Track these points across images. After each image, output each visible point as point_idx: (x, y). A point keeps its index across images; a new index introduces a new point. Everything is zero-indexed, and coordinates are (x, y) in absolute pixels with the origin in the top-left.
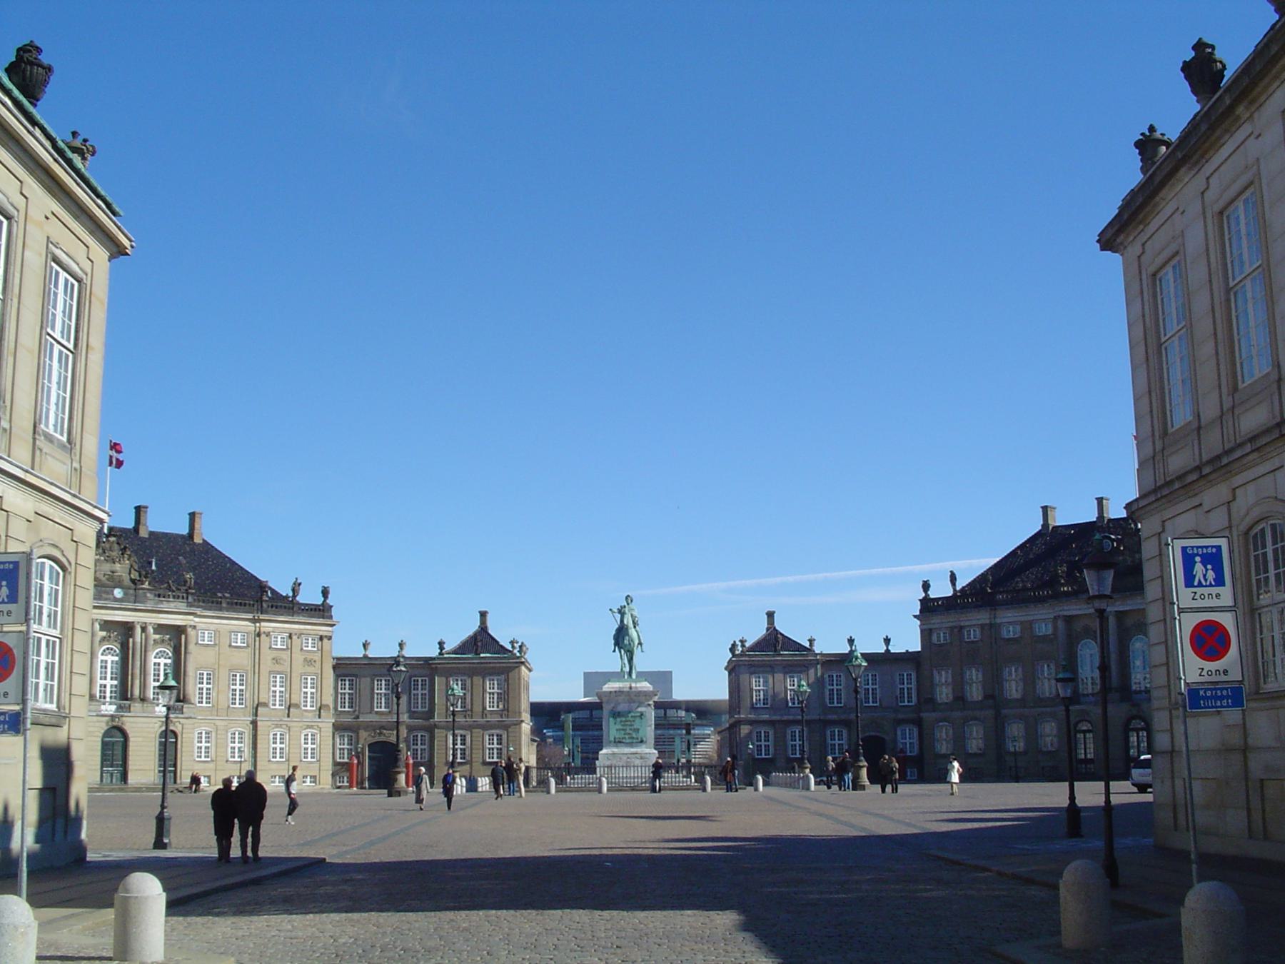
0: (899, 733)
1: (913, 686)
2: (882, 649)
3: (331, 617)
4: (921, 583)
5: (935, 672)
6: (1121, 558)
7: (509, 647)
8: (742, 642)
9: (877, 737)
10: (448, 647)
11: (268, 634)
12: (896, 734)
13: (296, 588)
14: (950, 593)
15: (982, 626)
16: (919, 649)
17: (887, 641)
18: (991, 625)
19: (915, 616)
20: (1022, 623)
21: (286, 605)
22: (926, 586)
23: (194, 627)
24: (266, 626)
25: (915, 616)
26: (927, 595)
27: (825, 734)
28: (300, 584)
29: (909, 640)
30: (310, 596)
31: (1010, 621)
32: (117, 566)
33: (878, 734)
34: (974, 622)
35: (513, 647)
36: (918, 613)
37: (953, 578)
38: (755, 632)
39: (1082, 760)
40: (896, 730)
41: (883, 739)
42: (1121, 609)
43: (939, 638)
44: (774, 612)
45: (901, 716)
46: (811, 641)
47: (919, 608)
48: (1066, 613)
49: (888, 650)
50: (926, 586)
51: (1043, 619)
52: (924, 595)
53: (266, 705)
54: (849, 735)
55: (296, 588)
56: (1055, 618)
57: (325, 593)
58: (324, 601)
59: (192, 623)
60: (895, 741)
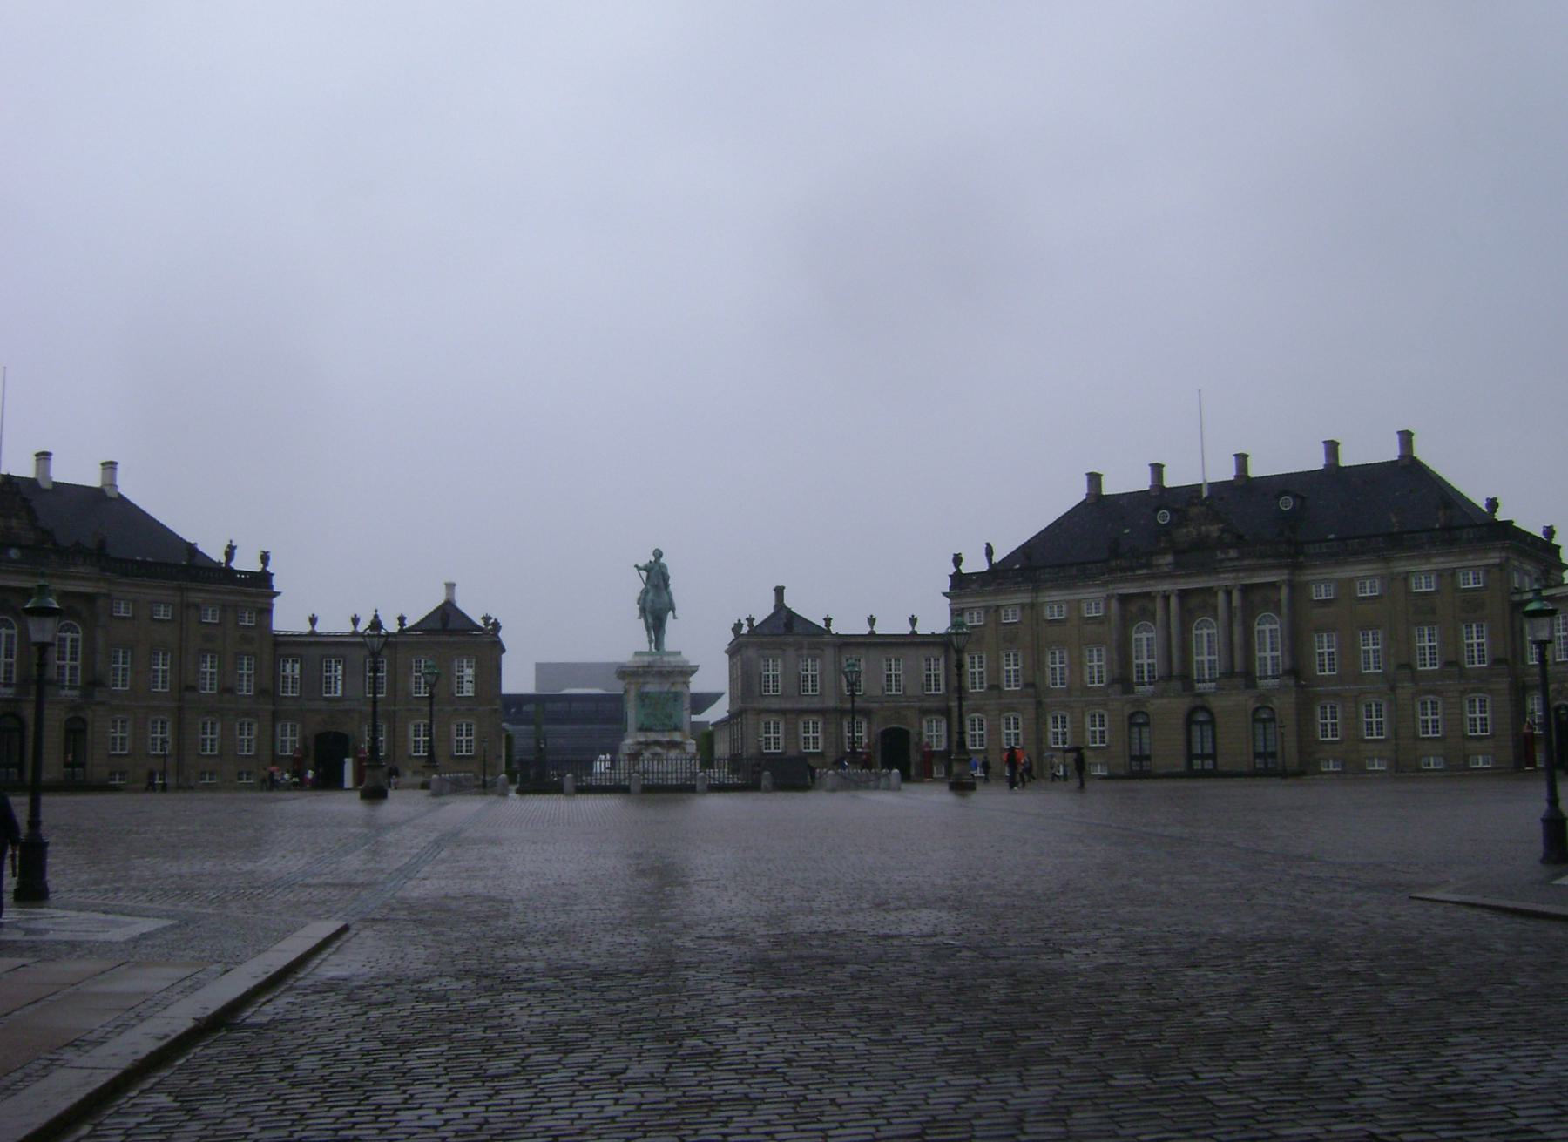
0: (925, 724)
3: (272, 587)
4: (952, 557)
6: (1185, 530)
7: (481, 623)
8: (750, 620)
10: (409, 623)
11: (197, 607)
12: (921, 728)
13: (230, 552)
14: (983, 566)
15: (1023, 606)
18: (1033, 606)
19: (944, 594)
20: (1068, 602)
21: (222, 574)
22: (957, 560)
23: (107, 596)
24: (195, 597)
25: (944, 594)
26: (959, 571)
27: (842, 724)
28: (235, 548)
29: (936, 620)
30: (246, 562)
31: (1055, 603)
32: (14, 523)
33: (902, 726)
34: (1015, 601)
35: (486, 624)
36: (948, 590)
37: (989, 551)
38: (763, 610)
40: (921, 723)
42: (1184, 587)
43: (974, 620)
44: (784, 588)
45: (926, 704)
46: (828, 621)
48: (1120, 592)
49: (914, 633)
50: (957, 560)
51: (1092, 600)
52: (954, 570)
53: (193, 688)
54: (869, 728)
55: (230, 552)
56: (1109, 597)
57: (265, 558)
58: (264, 569)
59: (104, 591)
60: (920, 734)
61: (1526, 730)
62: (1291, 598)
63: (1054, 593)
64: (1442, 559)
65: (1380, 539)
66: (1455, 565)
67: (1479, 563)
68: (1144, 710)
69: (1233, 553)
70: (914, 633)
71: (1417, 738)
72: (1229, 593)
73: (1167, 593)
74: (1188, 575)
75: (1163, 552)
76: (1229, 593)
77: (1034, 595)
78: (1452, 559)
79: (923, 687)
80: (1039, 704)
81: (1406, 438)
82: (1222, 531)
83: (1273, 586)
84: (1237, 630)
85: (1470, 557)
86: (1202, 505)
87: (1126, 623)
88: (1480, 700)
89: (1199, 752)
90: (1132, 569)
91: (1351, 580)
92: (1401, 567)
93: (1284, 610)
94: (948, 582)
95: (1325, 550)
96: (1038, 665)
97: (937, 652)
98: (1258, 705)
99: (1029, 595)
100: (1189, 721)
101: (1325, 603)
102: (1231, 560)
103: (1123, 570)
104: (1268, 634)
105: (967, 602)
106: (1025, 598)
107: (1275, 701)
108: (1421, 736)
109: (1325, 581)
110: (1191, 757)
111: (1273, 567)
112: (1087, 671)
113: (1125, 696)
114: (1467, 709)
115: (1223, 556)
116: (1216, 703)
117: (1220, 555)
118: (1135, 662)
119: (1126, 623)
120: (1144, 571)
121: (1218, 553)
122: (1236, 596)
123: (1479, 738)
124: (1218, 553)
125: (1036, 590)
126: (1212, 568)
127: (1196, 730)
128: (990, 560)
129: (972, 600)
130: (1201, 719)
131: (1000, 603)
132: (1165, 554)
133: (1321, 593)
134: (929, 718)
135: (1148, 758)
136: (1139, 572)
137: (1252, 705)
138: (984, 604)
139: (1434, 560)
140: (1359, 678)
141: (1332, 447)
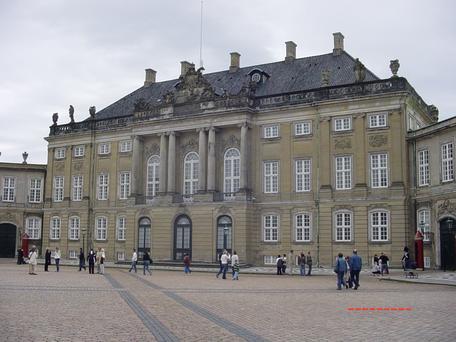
1: (41, 189)
2: (21, 161)
5: (55, 180)
6: (184, 92)
9: (13, 225)
12: (24, 224)
14: (68, 121)
15: (86, 146)
16: (46, 164)
17: (25, 155)
22: (55, 117)
25: (45, 138)
26: (55, 124)
33: (12, 223)
36: (48, 136)
39: (141, 248)
40: (24, 221)
41: (16, 227)
45: (29, 210)
47: (49, 133)
49: (25, 163)
50: (55, 117)
52: (53, 123)
61: (416, 238)
62: (249, 137)
63: (104, 137)
64: (357, 107)
65: (313, 93)
66: (366, 110)
67: (383, 108)
68: (147, 216)
69: (211, 105)
70: (25, 163)
71: (334, 243)
72: (207, 133)
73: (167, 134)
74: (181, 121)
75: (165, 106)
76: (207, 133)
77: (93, 138)
78: (364, 106)
79: (28, 198)
80: (90, 210)
81: (339, 38)
82: (205, 90)
83: (236, 128)
84: (211, 160)
85: (377, 104)
86: (195, 74)
87: (143, 156)
88: (382, 214)
89: (181, 247)
90: (148, 118)
91: (291, 123)
92: (326, 113)
93: (242, 144)
94: (49, 131)
95: (274, 102)
96: (92, 184)
97: (40, 176)
98: (221, 214)
99: (90, 138)
100: (176, 225)
101: (272, 140)
102: (209, 109)
103: (141, 119)
104: (232, 163)
105: (57, 144)
106: (87, 140)
107: (233, 212)
108: (337, 241)
109: (274, 125)
110: (176, 250)
111: (237, 113)
112: (119, 188)
113: (137, 206)
114: (372, 221)
115: (204, 107)
116: (194, 212)
117: (203, 107)
118: (148, 183)
119: (143, 156)
120: (155, 119)
121: (201, 105)
122: (211, 134)
123: (381, 244)
124: (201, 105)
125: (94, 135)
126: (198, 115)
127: (180, 230)
128: (72, 116)
129: (60, 142)
130: (184, 223)
131: (74, 144)
132: (167, 107)
133: (270, 133)
134: (30, 218)
135: (149, 250)
136: (151, 120)
137: (216, 214)
138: (65, 145)
139: (351, 107)
140: (294, 195)
141: (291, 46)
